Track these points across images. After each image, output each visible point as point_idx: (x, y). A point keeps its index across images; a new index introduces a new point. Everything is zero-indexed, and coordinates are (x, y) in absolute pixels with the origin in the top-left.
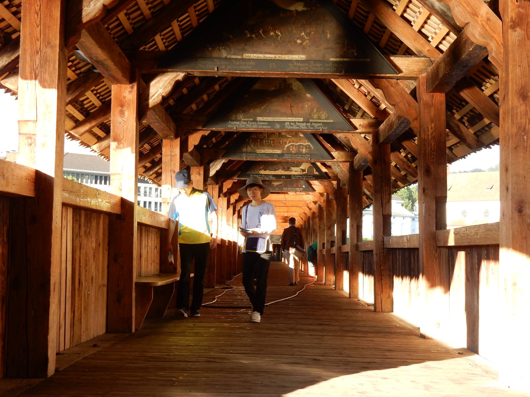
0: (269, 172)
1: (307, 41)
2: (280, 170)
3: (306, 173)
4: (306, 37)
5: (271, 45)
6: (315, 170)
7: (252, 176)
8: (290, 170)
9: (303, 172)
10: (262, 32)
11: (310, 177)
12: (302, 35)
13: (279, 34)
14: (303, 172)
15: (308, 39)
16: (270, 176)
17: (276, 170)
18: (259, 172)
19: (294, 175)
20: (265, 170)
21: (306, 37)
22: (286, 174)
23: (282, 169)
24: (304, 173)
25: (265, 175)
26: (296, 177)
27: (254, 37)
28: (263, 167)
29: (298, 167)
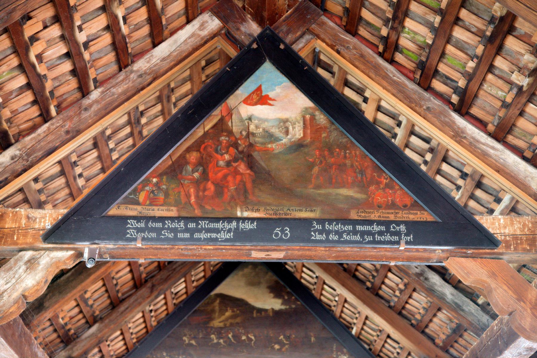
1: (287, 346)
4: (285, 341)
5: (243, 352)
10: (233, 336)
12: (280, 338)
13: (253, 338)
15: (287, 344)
21: (285, 341)
27: (222, 343)
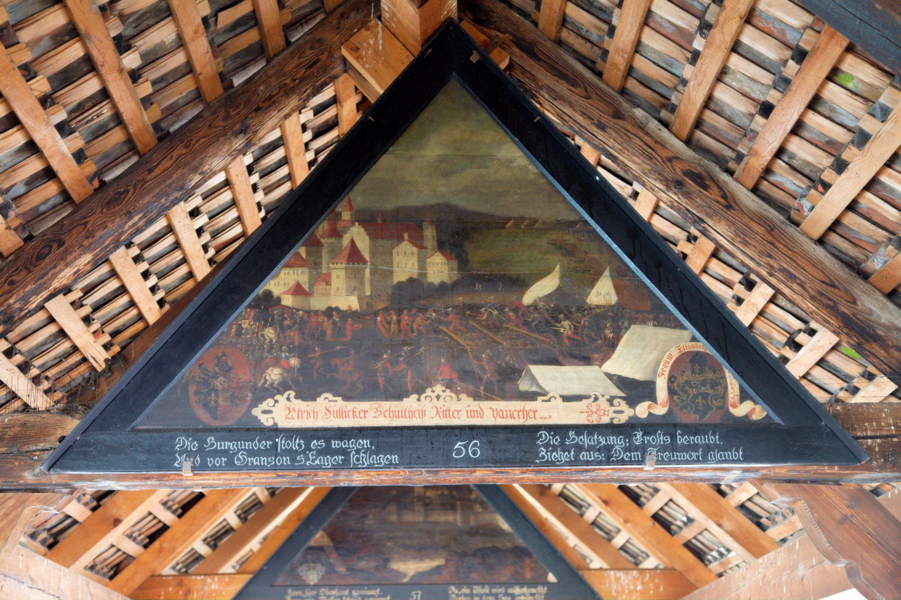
0: (340, 414)
2: (439, 389)
3: (660, 410)
6: (733, 384)
7: (193, 446)
8: (524, 385)
9: (632, 403)
11: (698, 440)
14: (632, 403)
16: (351, 445)
17: (399, 396)
18: (256, 412)
19: (560, 430)
20: (308, 394)
22: (488, 420)
23: (449, 386)
24: (642, 410)
25: (308, 434)
26: (579, 448)
28: (288, 370)
29: (586, 360)
